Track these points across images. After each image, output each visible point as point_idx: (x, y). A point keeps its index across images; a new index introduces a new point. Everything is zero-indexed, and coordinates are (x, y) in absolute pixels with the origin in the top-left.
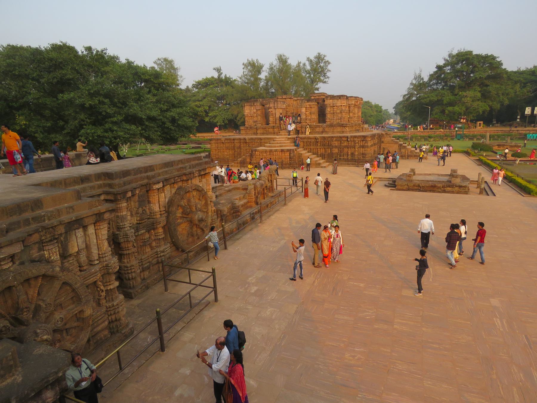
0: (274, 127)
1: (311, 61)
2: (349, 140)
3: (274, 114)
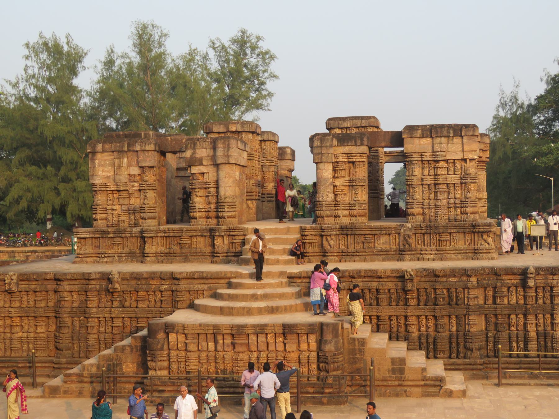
0: (211, 230)
1: (224, 48)
2: (531, 283)
3: (212, 185)
